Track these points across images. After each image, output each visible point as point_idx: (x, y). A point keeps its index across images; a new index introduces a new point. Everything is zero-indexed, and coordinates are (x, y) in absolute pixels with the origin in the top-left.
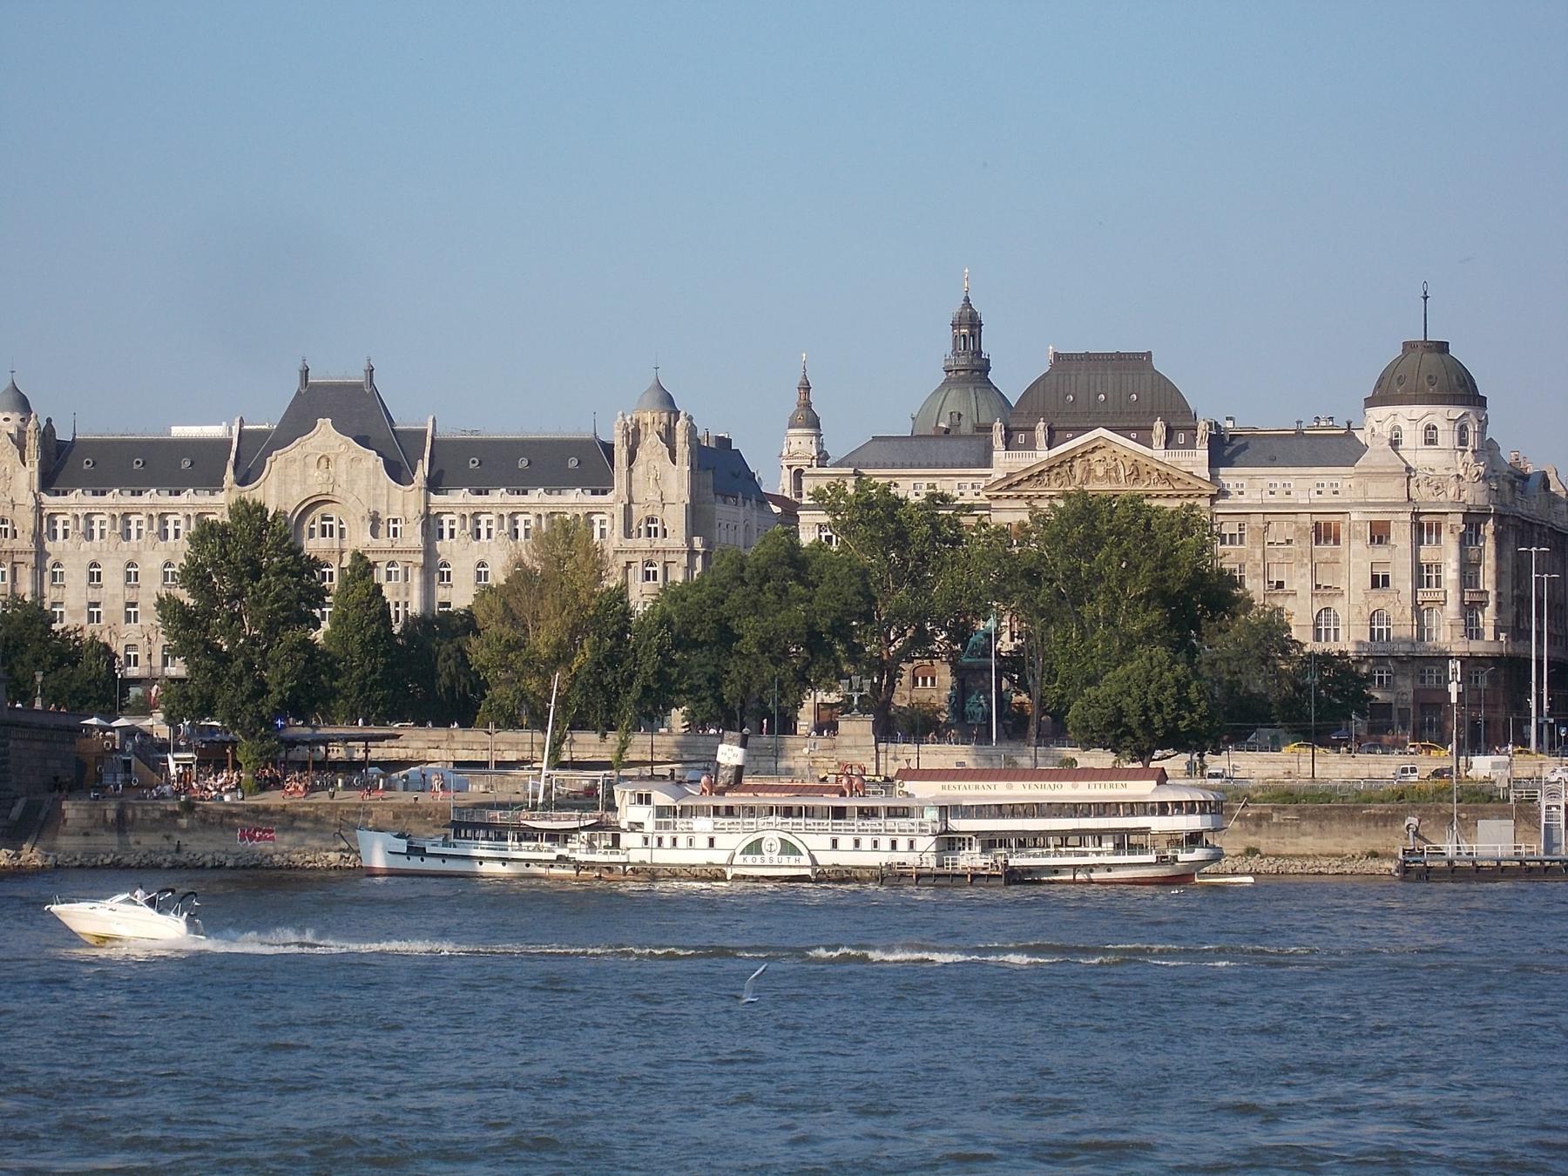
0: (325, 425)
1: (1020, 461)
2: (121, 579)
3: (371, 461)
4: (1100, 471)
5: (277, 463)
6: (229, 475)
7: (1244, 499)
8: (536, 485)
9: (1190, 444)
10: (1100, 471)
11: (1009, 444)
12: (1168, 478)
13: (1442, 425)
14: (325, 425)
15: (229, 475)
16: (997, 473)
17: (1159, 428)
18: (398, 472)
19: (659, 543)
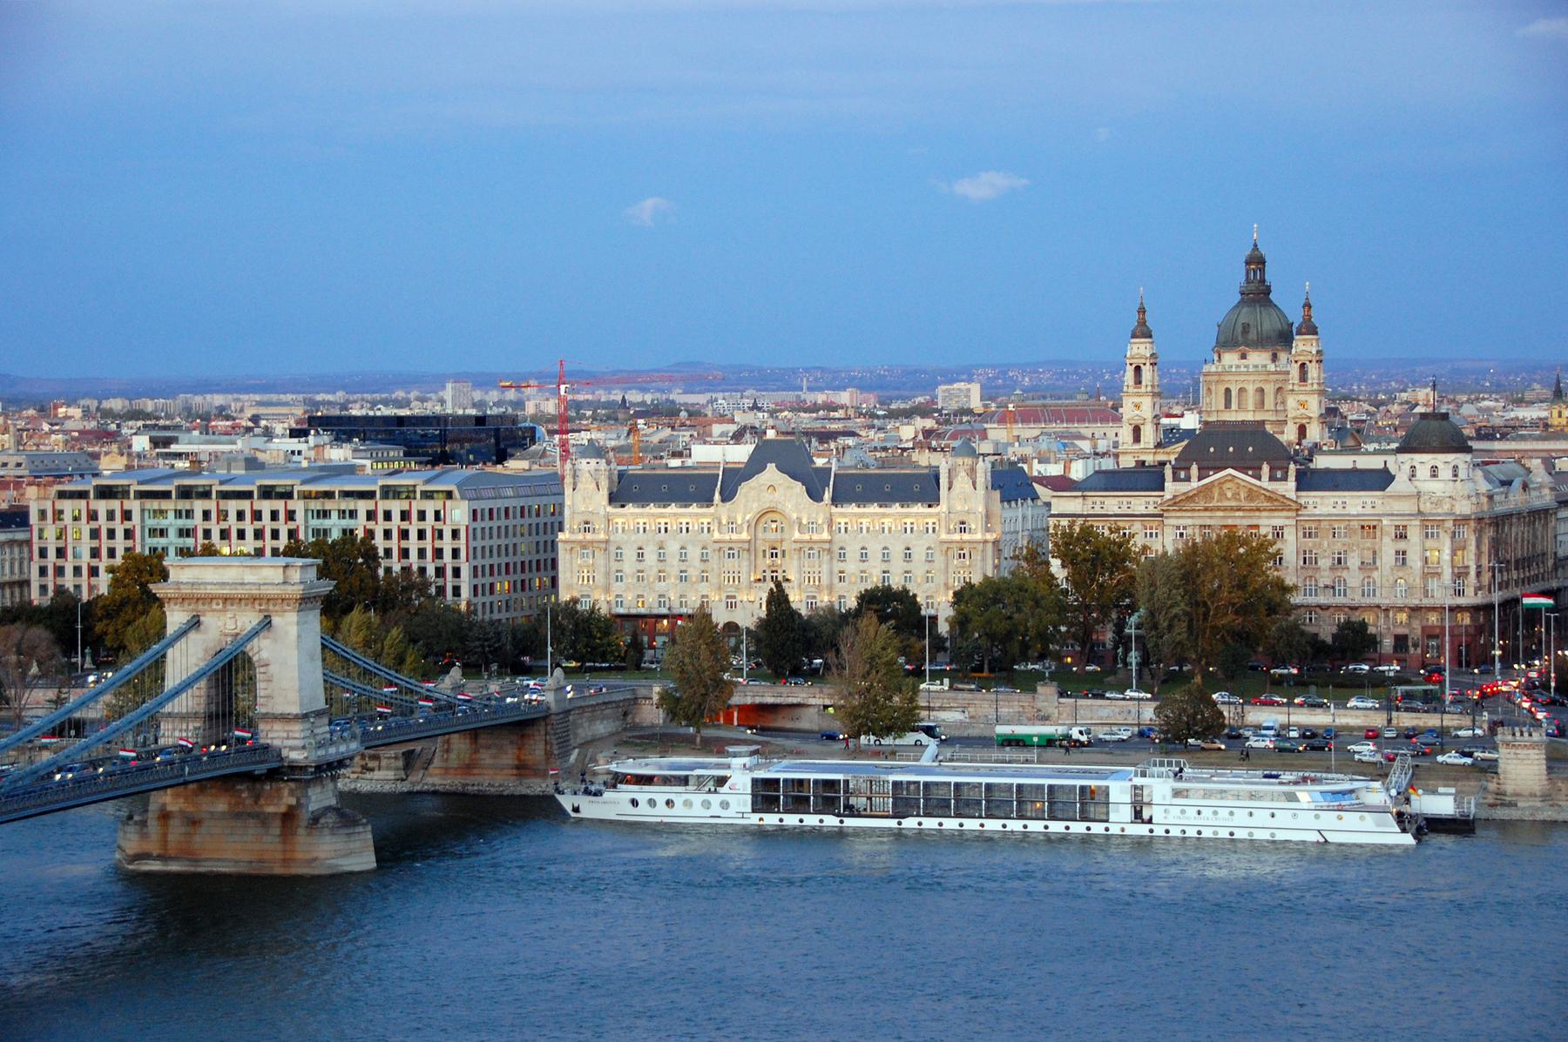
0: (771, 467)
1: (1183, 487)
2: (655, 557)
3: (799, 488)
4: (1229, 495)
5: (744, 489)
6: (717, 497)
7: (1317, 511)
8: (895, 501)
9: (1285, 478)
10: (1229, 495)
11: (1176, 479)
12: (1269, 499)
13: (1440, 466)
14: (771, 467)
15: (717, 497)
16: (1168, 495)
17: (1266, 468)
18: (815, 495)
19: (966, 537)
